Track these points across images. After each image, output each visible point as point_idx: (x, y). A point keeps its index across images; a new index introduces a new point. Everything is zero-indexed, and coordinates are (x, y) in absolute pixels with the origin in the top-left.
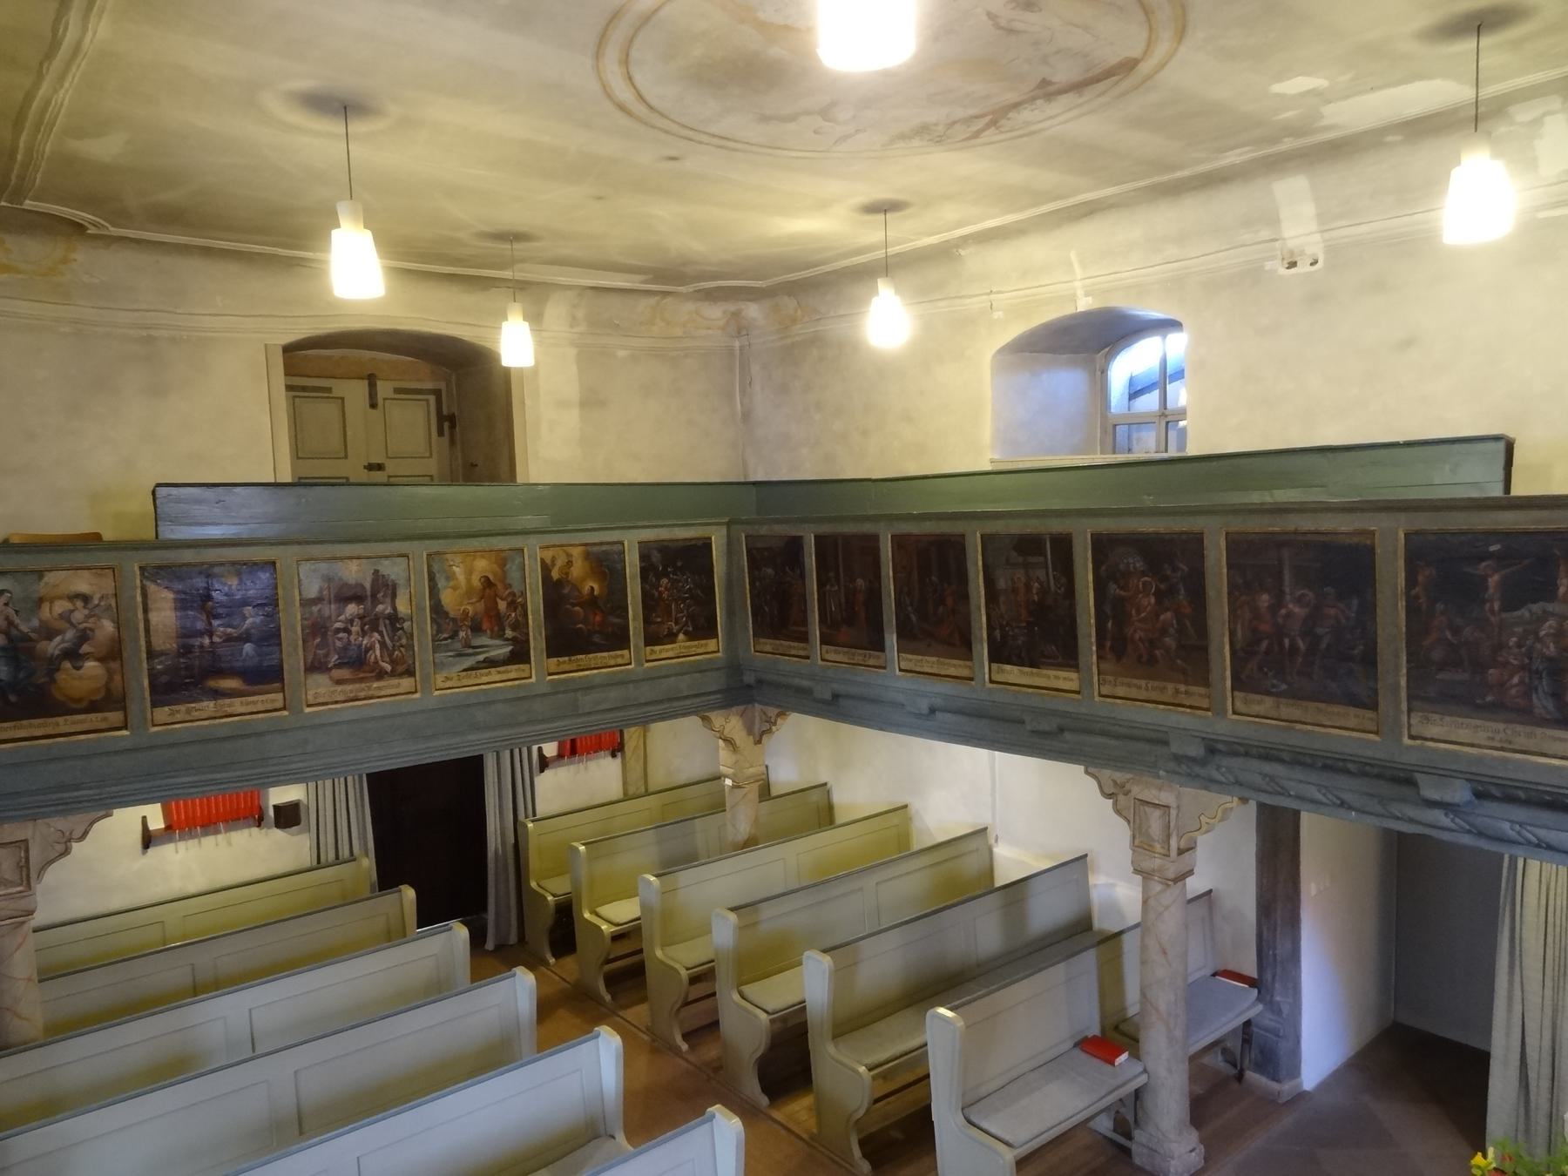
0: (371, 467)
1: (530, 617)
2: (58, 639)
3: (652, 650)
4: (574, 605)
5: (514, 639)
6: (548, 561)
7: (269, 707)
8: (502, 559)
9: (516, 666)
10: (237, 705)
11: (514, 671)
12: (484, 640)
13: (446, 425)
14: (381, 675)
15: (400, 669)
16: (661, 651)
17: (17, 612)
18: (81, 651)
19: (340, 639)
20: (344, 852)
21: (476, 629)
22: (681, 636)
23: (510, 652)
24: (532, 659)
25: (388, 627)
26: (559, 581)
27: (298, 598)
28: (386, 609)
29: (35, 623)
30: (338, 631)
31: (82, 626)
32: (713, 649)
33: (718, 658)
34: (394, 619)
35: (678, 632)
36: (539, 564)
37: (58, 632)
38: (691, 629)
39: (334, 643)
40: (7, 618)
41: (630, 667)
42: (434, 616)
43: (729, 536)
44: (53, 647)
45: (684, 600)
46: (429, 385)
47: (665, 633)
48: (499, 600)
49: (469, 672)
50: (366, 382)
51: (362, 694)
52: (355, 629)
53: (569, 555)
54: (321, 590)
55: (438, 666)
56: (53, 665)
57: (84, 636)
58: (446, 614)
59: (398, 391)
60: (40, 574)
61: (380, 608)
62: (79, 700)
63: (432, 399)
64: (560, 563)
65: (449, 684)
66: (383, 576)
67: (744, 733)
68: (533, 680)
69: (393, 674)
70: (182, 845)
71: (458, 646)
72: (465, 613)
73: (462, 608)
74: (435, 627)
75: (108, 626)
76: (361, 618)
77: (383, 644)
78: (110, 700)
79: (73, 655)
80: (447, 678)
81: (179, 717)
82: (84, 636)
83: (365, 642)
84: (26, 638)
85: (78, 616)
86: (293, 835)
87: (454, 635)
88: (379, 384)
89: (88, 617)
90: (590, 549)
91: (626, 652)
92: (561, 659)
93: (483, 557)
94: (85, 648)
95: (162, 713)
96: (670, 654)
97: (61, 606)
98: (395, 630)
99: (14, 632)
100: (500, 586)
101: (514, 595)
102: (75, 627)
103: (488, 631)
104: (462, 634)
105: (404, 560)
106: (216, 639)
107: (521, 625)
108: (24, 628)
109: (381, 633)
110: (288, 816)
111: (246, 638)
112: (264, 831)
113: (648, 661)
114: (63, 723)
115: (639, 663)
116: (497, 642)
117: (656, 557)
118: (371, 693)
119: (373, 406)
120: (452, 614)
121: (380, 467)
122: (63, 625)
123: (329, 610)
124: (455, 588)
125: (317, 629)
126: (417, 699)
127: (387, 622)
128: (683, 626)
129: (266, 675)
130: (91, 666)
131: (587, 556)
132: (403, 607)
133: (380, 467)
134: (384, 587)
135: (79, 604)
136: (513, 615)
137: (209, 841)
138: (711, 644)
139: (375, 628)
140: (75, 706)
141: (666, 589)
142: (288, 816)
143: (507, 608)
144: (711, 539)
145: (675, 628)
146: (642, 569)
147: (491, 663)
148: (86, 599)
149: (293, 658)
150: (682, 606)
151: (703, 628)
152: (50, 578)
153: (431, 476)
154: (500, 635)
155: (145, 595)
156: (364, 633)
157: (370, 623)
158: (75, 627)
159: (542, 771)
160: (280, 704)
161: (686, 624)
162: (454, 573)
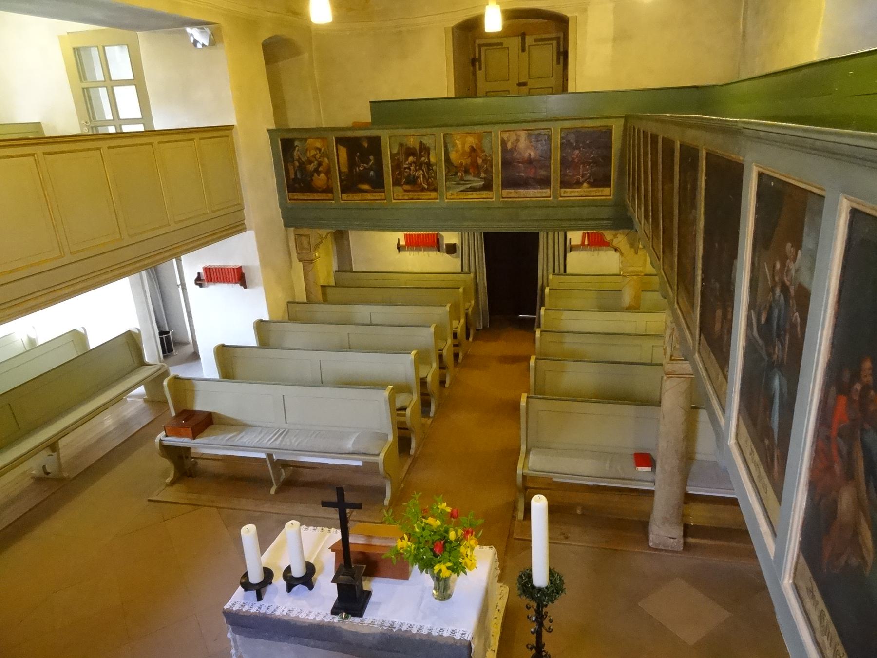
0: (521, 84)
1: (494, 167)
2: (312, 164)
3: (565, 191)
4: (519, 162)
5: (484, 178)
6: (506, 139)
7: (379, 198)
8: (480, 137)
9: (486, 192)
10: (369, 196)
11: (484, 194)
12: (470, 178)
13: (562, 58)
14: (423, 190)
15: (432, 187)
16: (571, 192)
18: (319, 170)
19: (406, 172)
20: (466, 269)
21: (466, 172)
22: (585, 185)
23: (483, 185)
24: (494, 189)
25: (426, 168)
26: (511, 149)
27: (389, 153)
28: (425, 159)
30: (405, 168)
32: (606, 193)
33: (609, 199)
34: (429, 164)
35: (583, 182)
36: (500, 140)
38: (592, 181)
39: (404, 173)
40: (298, 156)
41: (549, 199)
42: (446, 164)
43: (625, 125)
44: (311, 167)
45: (589, 164)
46: (554, 35)
47: (575, 182)
48: (478, 158)
49: (462, 193)
50: (520, 37)
51: (415, 197)
52: (412, 168)
53: (516, 134)
54: (398, 151)
55: (448, 188)
57: (320, 164)
58: (452, 164)
59: (536, 40)
60: (306, 140)
61: (423, 159)
62: (320, 188)
63: (555, 43)
64: (513, 138)
65: (452, 197)
66: (424, 144)
67: (628, 246)
68: (494, 200)
69: (428, 190)
70: (412, 253)
71: (458, 179)
72: (461, 164)
73: (460, 161)
74: (447, 170)
75: (326, 160)
76: (414, 162)
77: (424, 175)
78: (328, 190)
80: (452, 194)
81: (349, 199)
82: (320, 164)
83: (416, 174)
84: (304, 163)
85: (318, 156)
86: (453, 258)
87: (456, 174)
88: (527, 37)
90: (529, 131)
91: (548, 190)
92: (510, 191)
93: (470, 136)
94: (320, 169)
95: (345, 196)
96: (577, 194)
97: (313, 152)
98: (429, 169)
99: (300, 161)
100: (479, 151)
101: (486, 155)
103: (473, 174)
104: (459, 174)
105: (433, 136)
106: (361, 169)
107: (488, 171)
109: (423, 171)
110: (451, 249)
111: (370, 169)
112: (442, 253)
113: (561, 197)
114: (316, 196)
115: (555, 197)
116: (476, 179)
117: (572, 138)
118: (419, 197)
119: (523, 50)
120: (455, 163)
121: (525, 84)
122: (312, 159)
123: (402, 158)
124: (457, 151)
125: (397, 166)
126: (437, 202)
127: (426, 166)
128: (588, 178)
129: (378, 184)
130: (322, 175)
131: (529, 136)
132: (433, 160)
133: (525, 84)
134: (425, 149)
135: (318, 152)
136: (485, 166)
137: (421, 253)
138: (606, 191)
139: (420, 168)
140: (319, 190)
141: (577, 156)
142: (451, 249)
143: (482, 162)
144: (612, 126)
145: (581, 180)
146: (562, 144)
147: (473, 189)
148: (320, 150)
149: (388, 179)
150: (587, 167)
151: (602, 181)
152: (309, 141)
153: (551, 87)
154: (477, 175)
155: (337, 149)
156: (416, 170)
157: (419, 165)
158: (316, 160)
159: (570, 251)
160: (383, 198)
161: (589, 178)
162: (456, 144)
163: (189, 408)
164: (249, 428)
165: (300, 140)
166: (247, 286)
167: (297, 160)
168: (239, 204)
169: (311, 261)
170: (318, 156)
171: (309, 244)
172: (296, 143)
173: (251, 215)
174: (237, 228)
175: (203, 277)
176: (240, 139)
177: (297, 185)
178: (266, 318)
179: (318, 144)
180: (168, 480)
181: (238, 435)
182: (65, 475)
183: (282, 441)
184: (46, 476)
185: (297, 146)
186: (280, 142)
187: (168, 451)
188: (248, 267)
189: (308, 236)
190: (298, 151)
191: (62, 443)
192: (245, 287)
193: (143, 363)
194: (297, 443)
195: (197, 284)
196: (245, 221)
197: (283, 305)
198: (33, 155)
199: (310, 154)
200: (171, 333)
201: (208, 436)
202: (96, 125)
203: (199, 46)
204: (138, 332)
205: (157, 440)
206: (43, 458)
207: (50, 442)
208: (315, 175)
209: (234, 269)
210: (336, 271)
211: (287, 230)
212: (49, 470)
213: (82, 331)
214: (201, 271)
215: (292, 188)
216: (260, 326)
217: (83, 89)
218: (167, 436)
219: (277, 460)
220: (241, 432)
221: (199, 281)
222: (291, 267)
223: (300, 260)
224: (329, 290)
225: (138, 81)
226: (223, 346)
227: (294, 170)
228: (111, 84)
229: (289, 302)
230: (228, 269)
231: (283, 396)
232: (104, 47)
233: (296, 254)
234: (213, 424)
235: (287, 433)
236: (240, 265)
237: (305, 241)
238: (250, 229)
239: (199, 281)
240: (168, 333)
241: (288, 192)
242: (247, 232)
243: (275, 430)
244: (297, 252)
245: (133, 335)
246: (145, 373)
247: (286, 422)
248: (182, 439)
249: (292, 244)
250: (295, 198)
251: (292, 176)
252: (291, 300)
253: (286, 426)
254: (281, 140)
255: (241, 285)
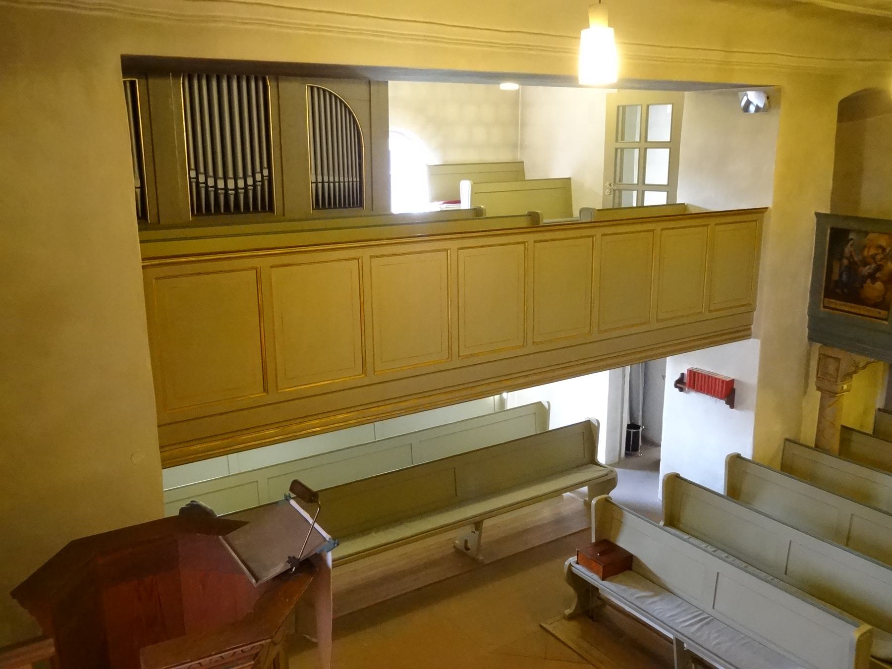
2: (868, 267)
17: (855, 250)
29: (860, 258)
31: (879, 263)
37: (870, 264)
44: (866, 270)
56: (864, 280)
57: (879, 268)
60: (867, 233)
79: (872, 277)
82: (879, 268)
84: (855, 263)
85: (879, 257)
89: (882, 259)
94: (878, 275)
97: (872, 251)
102: (875, 262)
108: (856, 259)
114: (863, 310)
130: (879, 285)
135: (880, 251)
148: (884, 249)
152: (871, 236)
158: (875, 262)
163: (612, 540)
164: (667, 593)
165: (859, 232)
166: (735, 406)
167: (847, 258)
168: (749, 304)
169: (834, 394)
170: (879, 257)
171: (837, 370)
172: (851, 236)
173: (762, 320)
174: (741, 333)
175: (686, 380)
176: (772, 226)
177: (838, 291)
178: (747, 454)
179: (883, 242)
180: (568, 612)
181: (652, 597)
182: (481, 558)
183: (698, 630)
184: (464, 551)
185: (852, 239)
186: (829, 231)
187: (574, 579)
188: (740, 383)
189: (838, 360)
190: (851, 246)
191: (487, 524)
192: (732, 406)
193: (594, 462)
194: (715, 642)
195: (676, 386)
196: (752, 326)
197: (777, 443)
198: (524, 243)
199: (868, 251)
200: (641, 429)
201: (619, 582)
202: (620, 188)
203: (752, 109)
204: (596, 424)
205: (567, 563)
206: (466, 532)
207: (478, 519)
208: (869, 281)
209: (723, 381)
210: (879, 410)
211: (810, 345)
212: (469, 545)
213: (546, 405)
214: (686, 372)
215: (829, 293)
216: (735, 463)
217: (616, 149)
218: (577, 563)
219: (688, 650)
220: (656, 595)
221: (680, 384)
222: (805, 392)
223: (819, 389)
224: (855, 437)
225: (673, 146)
226: (677, 476)
227: (840, 268)
228: (645, 145)
229: (787, 440)
230: (716, 379)
231: (718, 573)
232: (648, 106)
233: (816, 379)
234: (629, 568)
235: (707, 623)
236: (733, 378)
237: (832, 368)
238: (756, 337)
239: (680, 384)
240: (638, 427)
241: (825, 297)
242: (751, 339)
243: (697, 611)
244: (818, 377)
245: (592, 426)
246: (591, 473)
247: (713, 608)
248: (591, 574)
249: (814, 364)
250: (833, 306)
251: (835, 277)
252: (791, 438)
253: (709, 609)
254: (832, 229)
255: (727, 403)
